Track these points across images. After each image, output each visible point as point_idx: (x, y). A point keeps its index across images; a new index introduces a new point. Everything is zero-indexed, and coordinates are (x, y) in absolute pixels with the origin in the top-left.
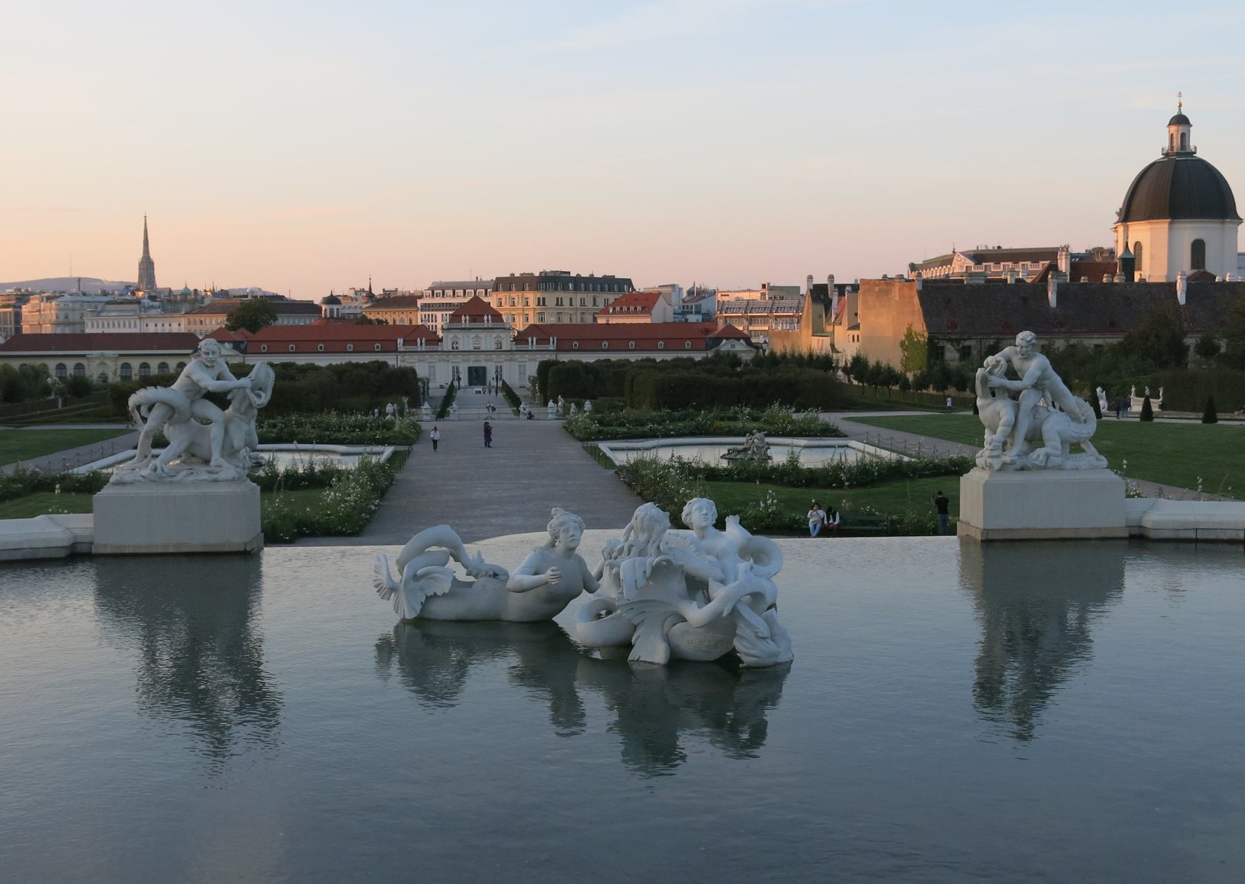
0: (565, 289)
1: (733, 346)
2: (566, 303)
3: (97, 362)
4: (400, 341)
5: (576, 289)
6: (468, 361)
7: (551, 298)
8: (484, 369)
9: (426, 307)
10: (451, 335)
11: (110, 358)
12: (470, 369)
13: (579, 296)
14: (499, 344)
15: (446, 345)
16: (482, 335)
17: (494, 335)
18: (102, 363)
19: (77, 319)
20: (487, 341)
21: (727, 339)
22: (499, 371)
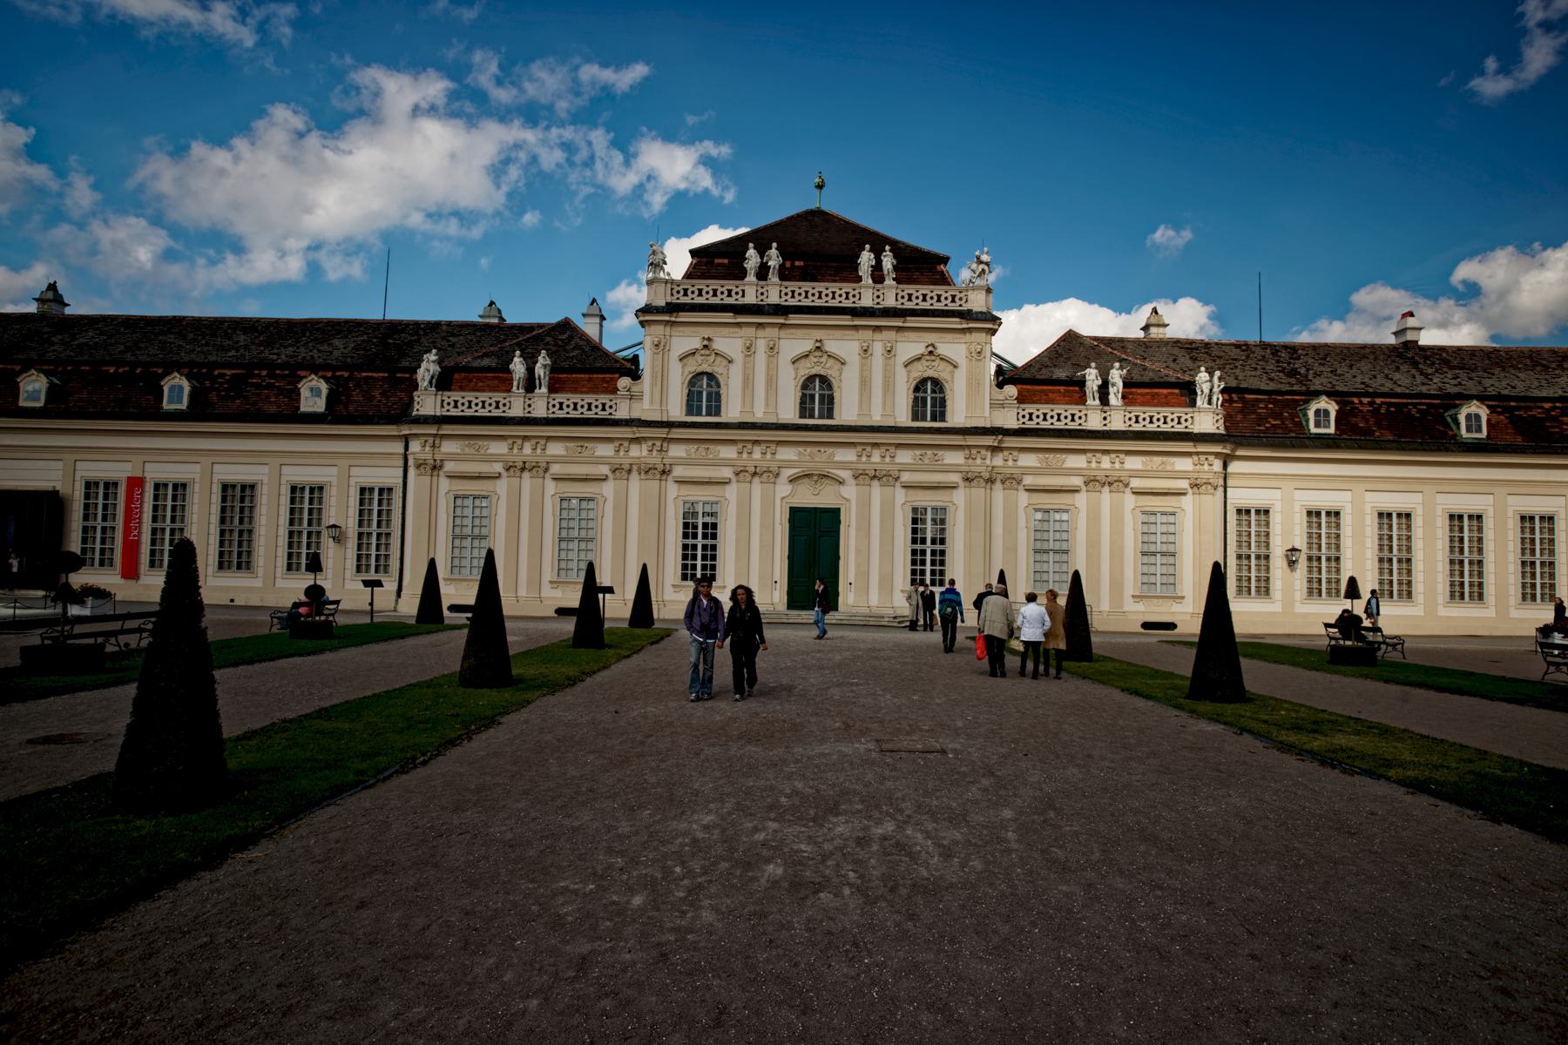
4: (429, 367)
10: (685, 341)
15: (660, 394)
16: (845, 345)
20: (872, 377)
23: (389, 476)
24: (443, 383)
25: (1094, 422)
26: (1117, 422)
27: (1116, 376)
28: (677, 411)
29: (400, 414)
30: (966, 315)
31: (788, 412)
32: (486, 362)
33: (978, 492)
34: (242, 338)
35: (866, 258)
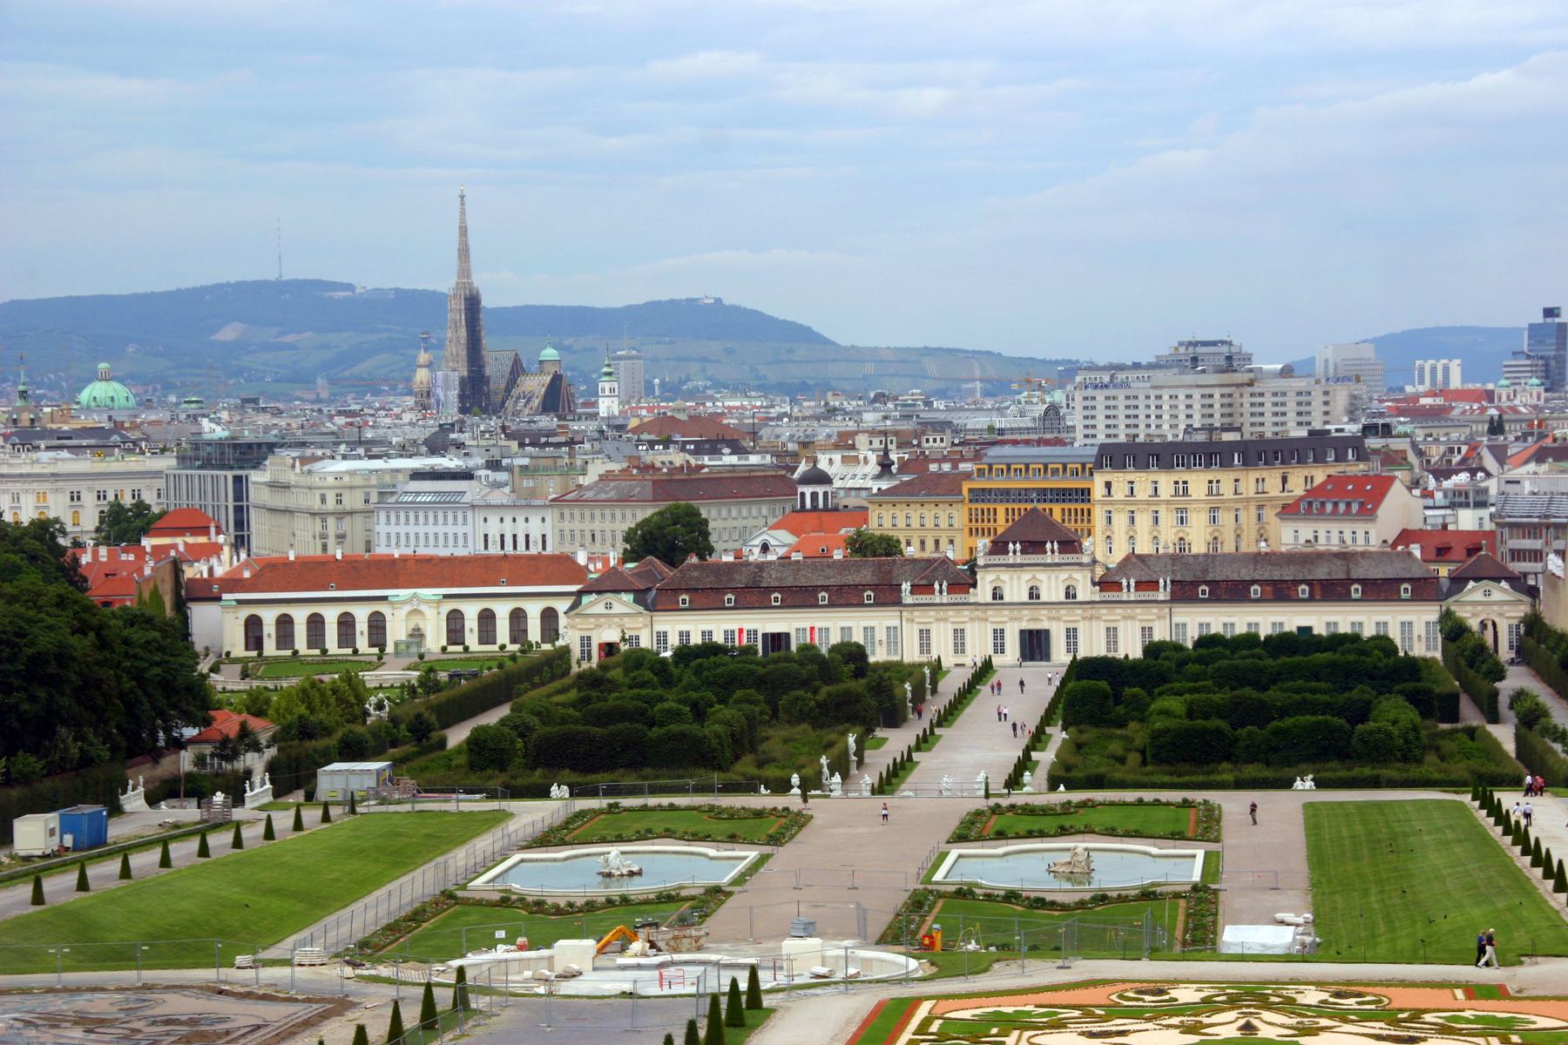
0: (1226, 464)
1: (1487, 593)
2: (1227, 489)
3: (407, 608)
4: (906, 586)
5: (1246, 463)
6: (1019, 619)
7: (1198, 482)
8: (1047, 632)
9: (978, 495)
11: (427, 602)
12: (1022, 632)
13: (1249, 481)
14: (1070, 593)
15: (983, 593)
17: (1064, 575)
18: (416, 612)
19: (360, 505)
20: (1052, 586)
21: (1477, 580)
22: (1072, 634)
23: (896, 623)
24: (912, 593)
25: (1125, 598)
26: (1132, 598)
27: (1133, 584)
28: (989, 599)
29: (898, 602)
30: (1080, 564)
31: (1025, 598)
32: (924, 582)
33: (1087, 623)
34: (830, 572)
35: (1048, 546)
